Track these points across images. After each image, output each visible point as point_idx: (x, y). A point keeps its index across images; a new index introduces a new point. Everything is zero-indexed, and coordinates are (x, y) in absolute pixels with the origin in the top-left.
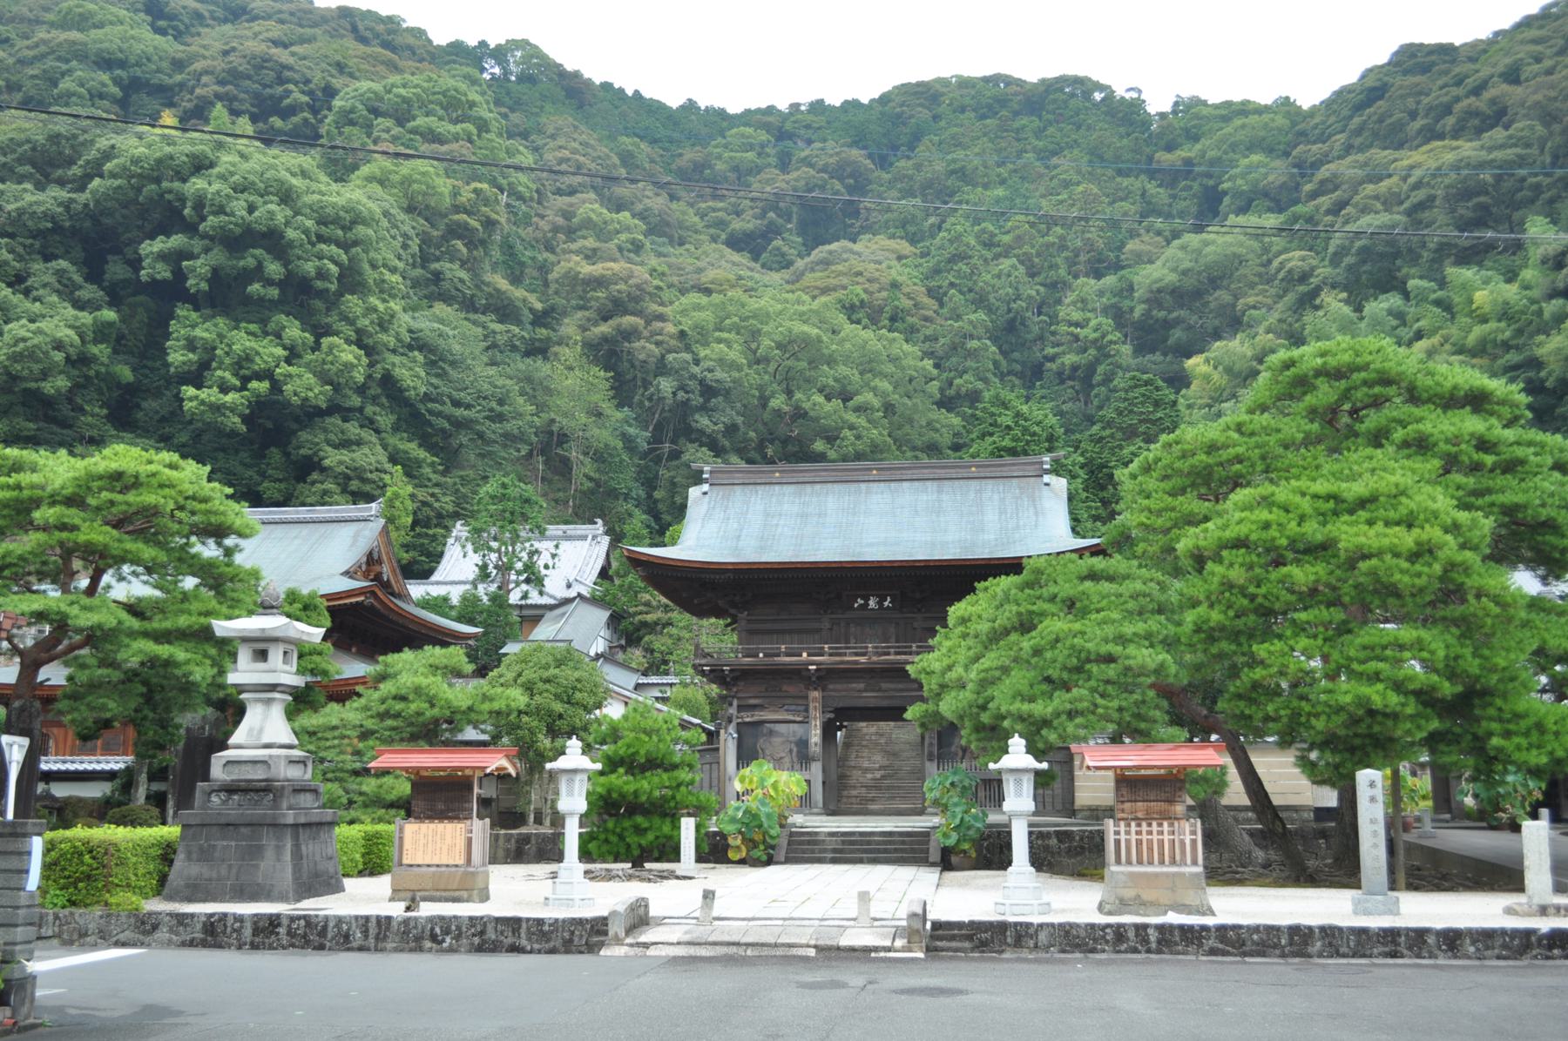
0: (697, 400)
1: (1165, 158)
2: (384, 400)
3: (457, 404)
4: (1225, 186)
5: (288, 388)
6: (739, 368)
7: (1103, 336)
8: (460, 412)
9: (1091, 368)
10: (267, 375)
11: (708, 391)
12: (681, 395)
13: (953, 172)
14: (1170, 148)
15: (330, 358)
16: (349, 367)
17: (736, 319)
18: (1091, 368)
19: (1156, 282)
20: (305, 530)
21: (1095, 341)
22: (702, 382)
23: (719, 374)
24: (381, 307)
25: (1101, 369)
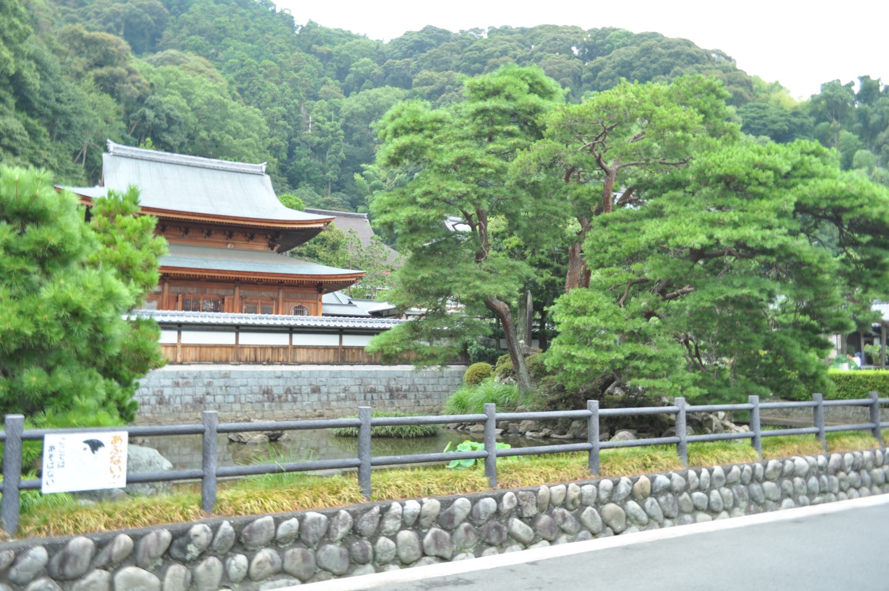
1: (320, 49)
2: (11, 88)
3: (58, 100)
4: (353, 69)
6: (186, 111)
7: (337, 130)
8: (58, 106)
9: (328, 146)
11: (170, 120)
12: (157, 120)
13: (219, 28)
14: (319, 43)
16: (6, 61)
17: (176, 83)
18: (328, 146)
20: (218, 174)
21: (332, 133)
22: (168, 116)
23: (177, 113)
24: (21, 26)
25: (334, 146)
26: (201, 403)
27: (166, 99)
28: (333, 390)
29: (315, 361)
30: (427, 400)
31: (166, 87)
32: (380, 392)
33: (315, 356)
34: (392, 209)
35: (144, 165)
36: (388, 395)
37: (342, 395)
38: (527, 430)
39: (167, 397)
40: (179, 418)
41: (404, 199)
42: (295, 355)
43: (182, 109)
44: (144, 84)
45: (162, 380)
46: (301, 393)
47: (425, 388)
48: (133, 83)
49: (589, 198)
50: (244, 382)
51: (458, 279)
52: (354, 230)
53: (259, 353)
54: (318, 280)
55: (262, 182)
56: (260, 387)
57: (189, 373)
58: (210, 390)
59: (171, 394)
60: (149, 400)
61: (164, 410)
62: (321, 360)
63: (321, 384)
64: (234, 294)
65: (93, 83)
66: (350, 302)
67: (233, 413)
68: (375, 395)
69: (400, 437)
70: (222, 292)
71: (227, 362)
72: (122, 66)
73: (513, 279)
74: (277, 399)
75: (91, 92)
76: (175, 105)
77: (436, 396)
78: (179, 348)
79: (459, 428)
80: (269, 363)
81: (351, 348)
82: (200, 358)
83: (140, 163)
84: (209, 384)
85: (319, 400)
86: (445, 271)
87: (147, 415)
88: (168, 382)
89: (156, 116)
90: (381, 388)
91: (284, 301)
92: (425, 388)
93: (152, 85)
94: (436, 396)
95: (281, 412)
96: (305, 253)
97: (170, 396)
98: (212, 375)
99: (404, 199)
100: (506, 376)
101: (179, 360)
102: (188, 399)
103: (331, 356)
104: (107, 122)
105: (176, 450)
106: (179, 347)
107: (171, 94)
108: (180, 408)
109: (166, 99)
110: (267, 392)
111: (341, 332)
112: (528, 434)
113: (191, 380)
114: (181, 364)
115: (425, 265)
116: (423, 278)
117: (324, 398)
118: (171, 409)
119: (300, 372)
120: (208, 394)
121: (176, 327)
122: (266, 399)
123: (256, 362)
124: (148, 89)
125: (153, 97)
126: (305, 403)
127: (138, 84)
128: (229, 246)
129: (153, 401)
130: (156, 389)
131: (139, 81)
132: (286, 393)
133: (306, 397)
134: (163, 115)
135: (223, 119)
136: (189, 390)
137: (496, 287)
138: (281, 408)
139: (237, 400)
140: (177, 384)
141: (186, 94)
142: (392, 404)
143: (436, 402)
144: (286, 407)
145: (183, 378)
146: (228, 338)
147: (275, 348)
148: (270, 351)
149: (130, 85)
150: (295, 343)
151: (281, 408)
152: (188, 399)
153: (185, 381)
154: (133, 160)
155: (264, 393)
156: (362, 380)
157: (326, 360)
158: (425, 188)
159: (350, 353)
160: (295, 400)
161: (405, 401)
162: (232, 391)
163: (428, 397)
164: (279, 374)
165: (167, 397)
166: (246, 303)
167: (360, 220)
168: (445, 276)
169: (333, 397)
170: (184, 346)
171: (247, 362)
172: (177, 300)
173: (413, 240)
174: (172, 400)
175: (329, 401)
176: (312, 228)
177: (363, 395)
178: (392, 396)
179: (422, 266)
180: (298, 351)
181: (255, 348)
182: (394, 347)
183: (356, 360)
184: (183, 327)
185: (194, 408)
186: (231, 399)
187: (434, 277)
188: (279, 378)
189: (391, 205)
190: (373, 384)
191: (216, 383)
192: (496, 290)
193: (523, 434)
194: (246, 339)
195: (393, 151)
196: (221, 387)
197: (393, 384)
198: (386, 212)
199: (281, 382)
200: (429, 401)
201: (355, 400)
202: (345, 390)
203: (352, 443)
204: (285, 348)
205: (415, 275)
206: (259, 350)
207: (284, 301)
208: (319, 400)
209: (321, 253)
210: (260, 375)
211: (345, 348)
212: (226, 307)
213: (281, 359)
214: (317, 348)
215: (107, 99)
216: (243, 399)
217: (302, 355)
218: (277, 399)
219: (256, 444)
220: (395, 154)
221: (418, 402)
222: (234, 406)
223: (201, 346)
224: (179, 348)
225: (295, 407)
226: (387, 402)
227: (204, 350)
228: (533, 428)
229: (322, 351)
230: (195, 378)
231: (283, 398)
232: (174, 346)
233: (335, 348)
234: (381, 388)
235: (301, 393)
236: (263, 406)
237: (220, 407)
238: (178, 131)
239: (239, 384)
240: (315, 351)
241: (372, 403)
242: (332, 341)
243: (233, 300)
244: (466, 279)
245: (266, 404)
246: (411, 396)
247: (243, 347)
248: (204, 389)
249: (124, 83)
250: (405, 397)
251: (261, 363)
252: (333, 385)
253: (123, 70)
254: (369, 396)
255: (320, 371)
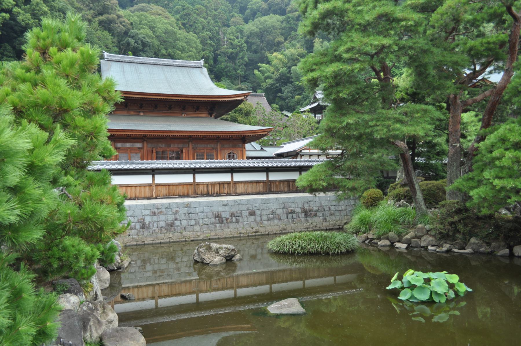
0: (141, 48)
4: (249, 6)
5: (20, 18)
6: (153, 38)
7: (242, 45)
9: (237, 54)
10: (8, 11)
11: (144, 44)
12: (136, 45)
15: (38, 8)
18: (237, 54)
19: (252, 30)
21: (239, 46)
22: (142, 41)
25: (241, 54)
26: (172, 226)
27: (140, 32)
28: (264, 213)
29: (250, 192)
30: (332, 217)
31: (140, 24)
32: (298, 213)
33: (250, 189)
34: (317, 67)
35: (126, 66)
36: (303, 214)
37: (271, 216)
38: (429, 244)
39: (147, 223)
40: (157, 238)
41: (326, 59)
42: (236, 188)
43: (150, 37)
44: (127, 23)
45: (143, 211)
46: (241, 216)
47: (329, 208)
48: (121, 23)
49: (483, 48)
50: (201, 209)
51: (378, 123)
52: (260, 102)
53: (210, 188)
54: (243, 135)
55: (202, 72)
56: (213, 212)
57: (162, 205)
58: (178, 217)
59: (150, 221)
60: (135, 226)
61: (146, 233)
62: (254, 191)
63: (256, 208)
64: (189, 147)
65: (98, 25)
66: (262, 149)
67: (195, 233)
68: (294, 215)
69: (328, 254)
70: (181, 146)
71: (188, 196)
72: (113, 14)
73: (426, 121)
74: (225, 221)
75: (97, 30)
76: (146, 35)
77: (338, 214)
78: (154, 187)
79: (367, 242)
80: (218, 195)
81: (275, 181)
82: (169, 193)
83: (123, 63)
84: (177, 212)
85: (255, 220)
86: (366, 117)
87: (134, 236)
88: (147, 212)
89: (135, 42)
90: (299, 210)
91: (221, 150)
92: (329, 208)
93: (132, 24)
94: (338, 214)
95: (229, 230)
96: (230, 119)
97: (150, 222)
98: (178, 206)
99: (326, 59)
100: (400, 200)
101: (154, 196)
102: (163, 224)
103: (261, 188)
104: (107, 48)
105: (156, 261)
106: (154, 186)
107: (143, 28)
108: (157, 231)
109: (140, 32)
110: (218, 216)
111: (267, 170)
112: (430, 248)
113: (164, 210)
114: (156, 198)
115: (348, 113)
116: (348, 124)
117: (258, 219)
118: (151, 232)
119: (241, 200)
120: (176, 219)
121: (151, 171)
122: (217, 221)
123: (208, 195)
124: (129, 26)
125: (133, 31)
126: (245, 223)
127: (124, 24)
128: (183, 115)
129: (138, 226)
130: (140, 218)
131: (124, 22)
132: (231, 216)
133: (245, 219)
134: (139, 41)
135: (175, 41)
136: (163, 218)
137: (414, 128)
138: (228, 228)
139: (197, 223)
140: (154, 214)
141: (152, 28)
142: (307, 221)
143: (338, 218)
144: (232, 226)
145: (158, 209)
146: (188, 178)
147: (221, 184)
148: (218, 186)
149: (119, 24)
150: (235, 179)
151: (228, 228)
152: (163, 224)
153: (159, 210)
154: (120, 63)
155: (216, 217)
156: (284, 205)
157: (258, 191)
158: (349, 45)
159: (275, 186)
160: (238, 222)
161: (316, 219)
162: (193, 216)
163: (332, 215)
164: (225, 203)
165: (147, 223)
166: (196, 152)
167: (260, 98)
168: (367, 122)
169: (265, 218)
170: (158, 185)
171: (202, 195)
172: (153, 153)
173: (338, 92)
174: (151, 225)
175: (262, 221)
176: (237, 100)
177: (286, 215)
178: (306, 215)
179: (344, 115)
180: (237, 185)
181: (207, 184)
182: (321, 182)
183: (279, 190)
184: (156, 171)
185: (167, 230)
186: (193, 222)
187: (357, 123)
188: (225, 205)
189: (316, 64)
190: (293, 207)
191: (182, 211)
192: (415, 131)
193: (426, 249)
194: (201, 178)
195: (318, 16)
196: (185, 214)
197: (306, 207)
198: (312, 70)
199: (227, 208)
200: (333, 218)
201: (280, 219)
202: (273, 212)
203: (289, 259)
204: (228, 183)
205: (341, 123)
206: (210, 186)
207: (221, 150)
208: (255, 220)
209: (239, 119)
210: (212, 204)
211: (271, 182)
212: (184, 155)
213: (226, 192)
214: (251, 182)
215: (106, 33)
216: (201, 222)
217: (240, 188)
218: (225, 221)
219: (216, 265)
220: (319, 19)
221: (325, 218)
222: (195, 227)
223: (169, 185)
224: (154, 187)
225: (238, 226)
226: (303, 220)
227: (171, 187)
228: (434, 243)
229: (255, 184)
230: (166, 208)
231: (230, 220)
232: (150, 185)
233: (263, 182)
234: (299, 210)
235: (241, 216)
236: (216, 226)
237: (185, 228)
238: (148, 50)
239: (197, 211)
240: (250, 185)
241: (293, 221)
242: (261, 177)
243: (188, 150)
244: (387, 123)
245: (218, 225)
246: (320, 214)
247: (199, 184)
248: (173, 216)
249: (116, 24)
250: (316, 215)
251: (212, 195)
252: (264, 209)
253: (114, 16)
254: (290, 216)
255: (254, 199)
